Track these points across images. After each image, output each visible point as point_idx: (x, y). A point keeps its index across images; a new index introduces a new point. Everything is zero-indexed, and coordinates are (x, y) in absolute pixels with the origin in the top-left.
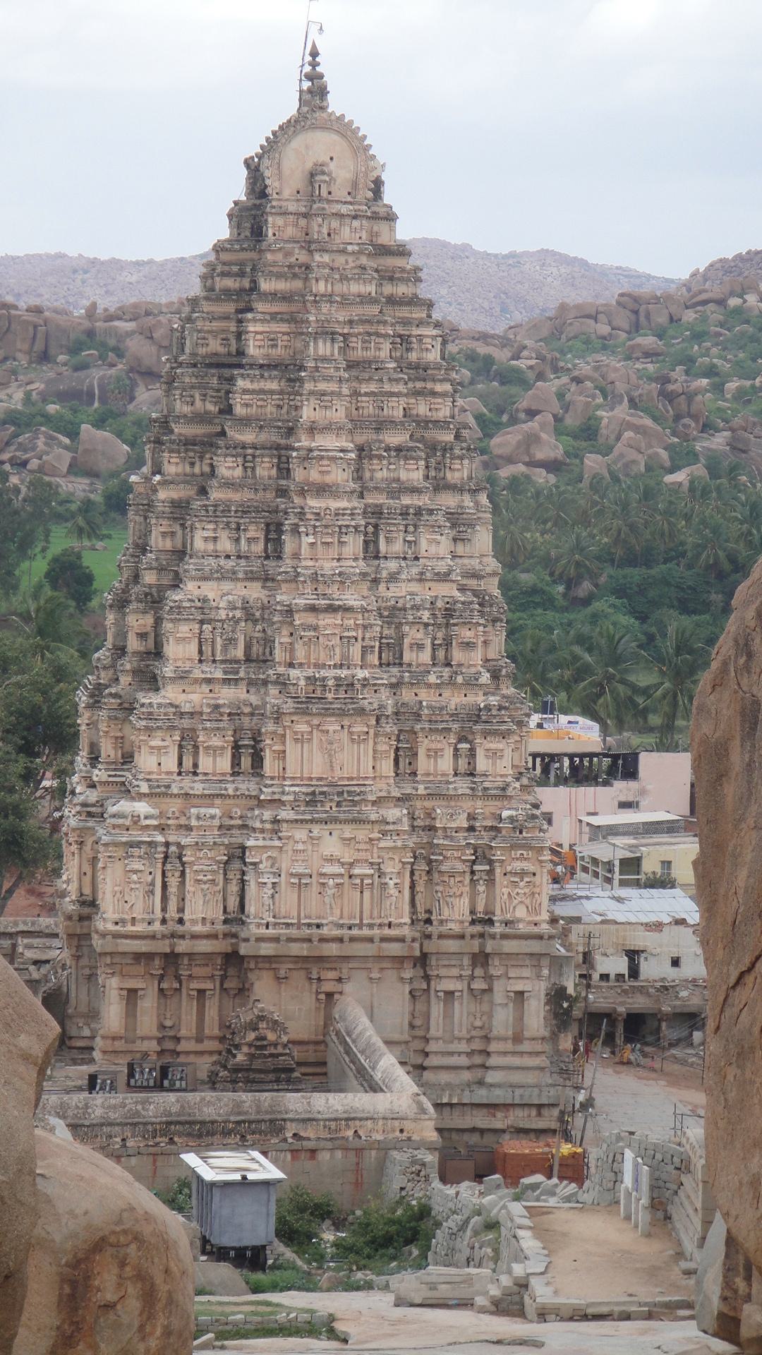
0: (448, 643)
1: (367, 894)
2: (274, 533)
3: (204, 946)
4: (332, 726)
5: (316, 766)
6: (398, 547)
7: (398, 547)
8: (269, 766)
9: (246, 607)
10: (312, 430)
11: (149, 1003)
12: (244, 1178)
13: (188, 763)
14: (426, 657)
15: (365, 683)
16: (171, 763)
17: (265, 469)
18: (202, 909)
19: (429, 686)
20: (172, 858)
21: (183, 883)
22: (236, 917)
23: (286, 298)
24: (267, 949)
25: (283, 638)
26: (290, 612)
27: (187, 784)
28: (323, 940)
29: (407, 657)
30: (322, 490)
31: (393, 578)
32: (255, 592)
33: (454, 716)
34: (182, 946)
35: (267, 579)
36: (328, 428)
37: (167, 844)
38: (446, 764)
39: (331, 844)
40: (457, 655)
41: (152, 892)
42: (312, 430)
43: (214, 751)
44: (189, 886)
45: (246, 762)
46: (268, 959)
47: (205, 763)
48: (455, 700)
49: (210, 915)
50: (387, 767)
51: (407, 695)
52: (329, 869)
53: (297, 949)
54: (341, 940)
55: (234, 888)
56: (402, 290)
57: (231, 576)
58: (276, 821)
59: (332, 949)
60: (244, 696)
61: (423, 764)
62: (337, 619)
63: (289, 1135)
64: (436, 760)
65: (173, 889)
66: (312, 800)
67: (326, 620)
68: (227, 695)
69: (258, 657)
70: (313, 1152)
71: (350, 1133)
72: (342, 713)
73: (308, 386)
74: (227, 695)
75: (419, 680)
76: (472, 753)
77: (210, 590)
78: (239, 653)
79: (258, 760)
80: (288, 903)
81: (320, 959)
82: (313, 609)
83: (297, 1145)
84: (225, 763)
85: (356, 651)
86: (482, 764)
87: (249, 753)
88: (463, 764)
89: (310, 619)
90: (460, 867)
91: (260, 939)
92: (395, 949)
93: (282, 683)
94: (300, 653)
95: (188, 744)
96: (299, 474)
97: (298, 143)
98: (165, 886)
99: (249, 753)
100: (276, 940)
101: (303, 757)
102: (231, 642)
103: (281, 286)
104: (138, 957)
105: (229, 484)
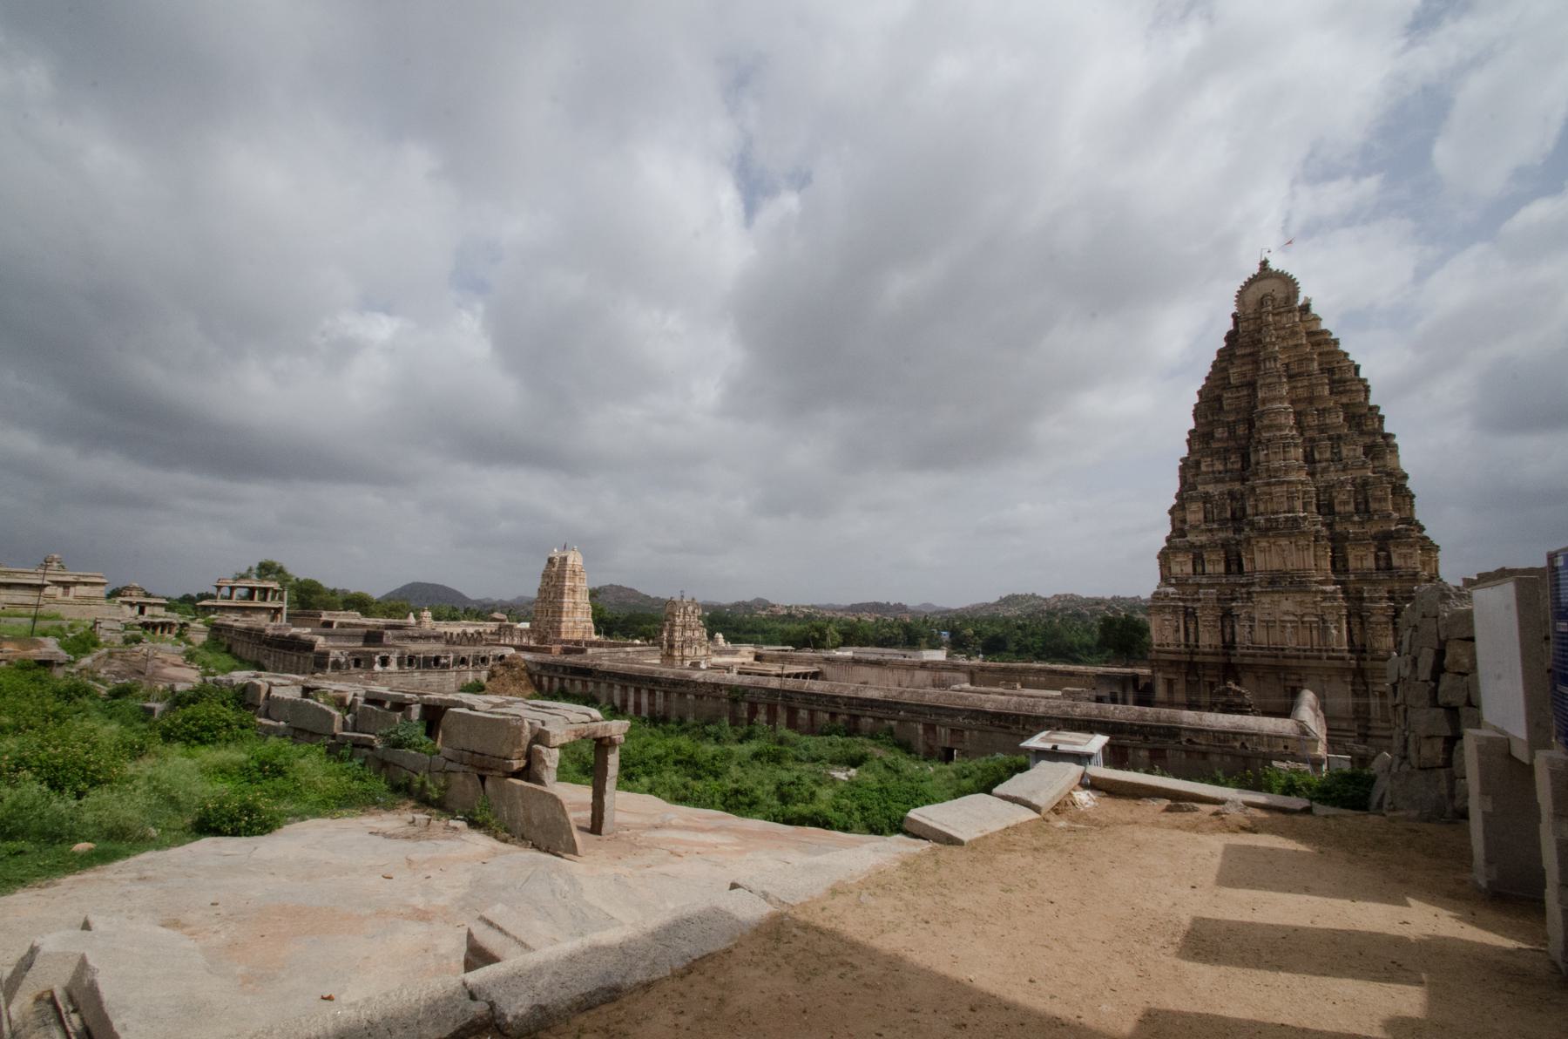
0: (1367, 502)
1: (1315, 633)
2: (1245, 458)
3: (1210, 659)
4: (1284, 542)
5: (1276, 563)
6: (1328, 455)
7: (1328, 455)
8: (1247, 567)
9: (1231, 494)
10: (1264, 402)
11: (1180, 686)
12: (1055, 748)
13: (1199, 569)
14: (1351, 508)
15: (1305, 518)
16: (1189, 569)
17: (1241, 430)
18: (1208, 639)
19: (1354, 523)
20: (1189, 614)
21: (1196, 628)
22: (1229, 645)
23: (1250, 354)
24: (1247, 660)
25: (1252, 501)
26: (1253, 489)
27: (1198, 579)
28: (1285, 657)
29: (1337, 509)
30: (1269, 428)
31: (1325, 470)
32: (1237, 486)
33: (1374, 537)
34: (1196, 659)
35: (1243, 480)
36: (1274, 399)
37: (1186, 608)
38: (1370, 563)
39: (1287, 605)
40: (1373, 506)
41: (1177, 630)
42: (1264, 402)
43: (1213, 562)
44: (1201, 629)
45: (1234, 568)
46: (1249, 665)
47: (1209, 568)
48: (1373, 529)
49: (1214, 643)
50: (1326, 564)
51: (1338, 528)
52: (1286, 618)
53: (1266, 661)
54: (1298, 657)
55: (1228, 630)
56: (1326, 349)
57: (1222, 481)
58: (1249, 593)
59: (1294, 662)
60: (1230, 534)
61: (1352, 564)
62: (1285, 488)
63: (1183, 740)
64: (1362, 559)
65: (1191, 630)
66: (1272, 582)
67: (1276, 490)
68: (1222, 535)
69: (1238, 519)
70: (1205, 755)
71: (1237, 744)
72: (1289, 536)
73: (1260, 382)
74: (1222, 535)
75: (1347, 518)
76: (1389, 558)
77: (1210, 488)
78: (1228, 515)
79: (1240, 566)
80: (1261, 636)
81: (1286, 668)
82: (1268, 484)
83: (1191, 747)
84: (1221, 568)
85: (1298, 504)
86: (1396, 561)
87: (1234, 563)
88: (1382, 563)
89: (1266, 489)
90: (1384, 619)
91: (1243, 655)
92: (1337, 663)
93: (1252, 524)
94: (1261, 508)
95: (1198, 560)
96: (1258, 424)
97: (1253, 288)
98: (1186, 630)
99: (1234, 563)
100: (1254, 656)
101: (1264, 558)
102: (1222, 509)
103: (1248, 351)
104: (1172, 663)
105: (1220, 440)
